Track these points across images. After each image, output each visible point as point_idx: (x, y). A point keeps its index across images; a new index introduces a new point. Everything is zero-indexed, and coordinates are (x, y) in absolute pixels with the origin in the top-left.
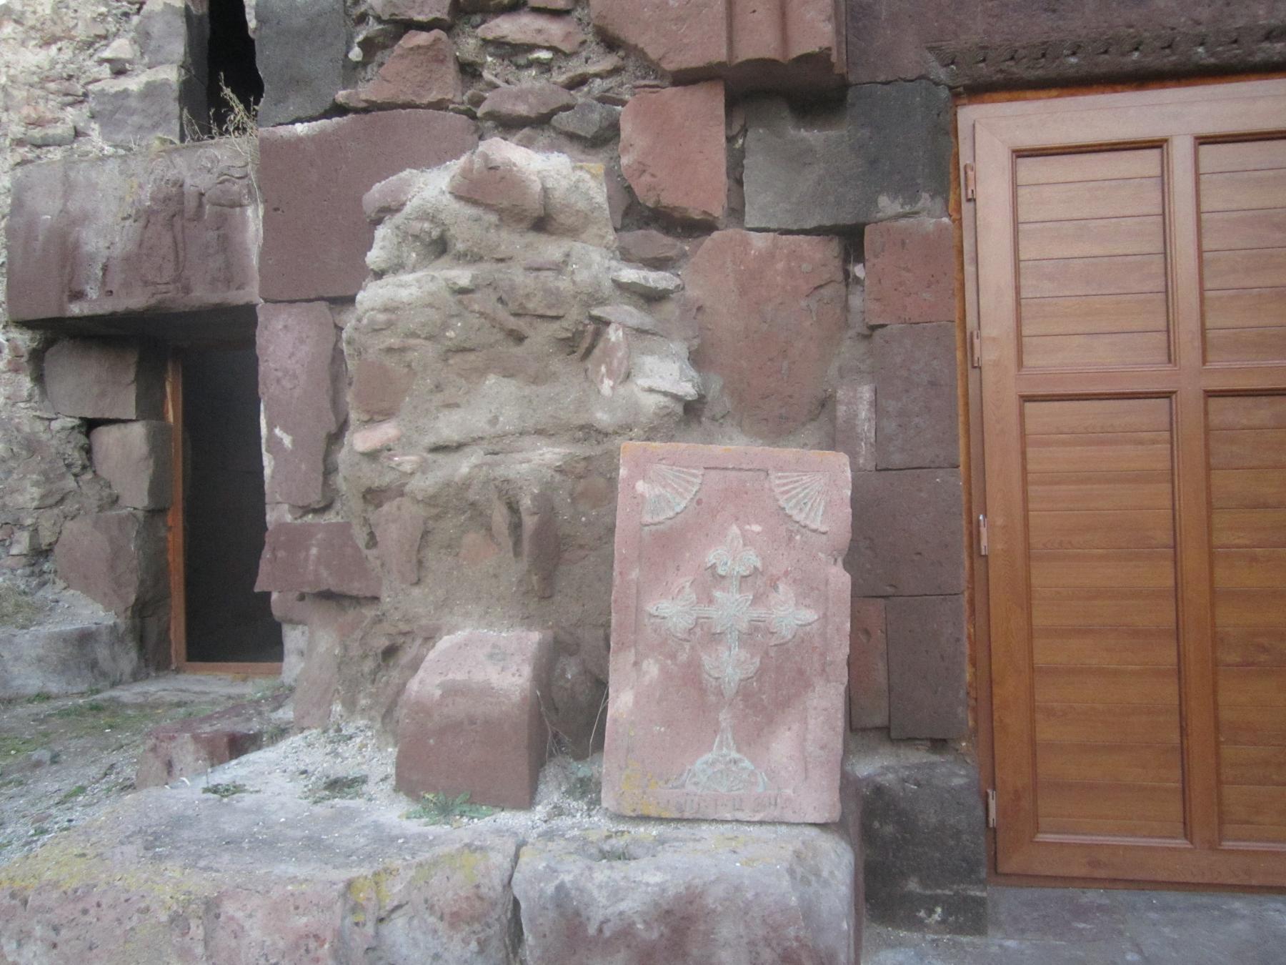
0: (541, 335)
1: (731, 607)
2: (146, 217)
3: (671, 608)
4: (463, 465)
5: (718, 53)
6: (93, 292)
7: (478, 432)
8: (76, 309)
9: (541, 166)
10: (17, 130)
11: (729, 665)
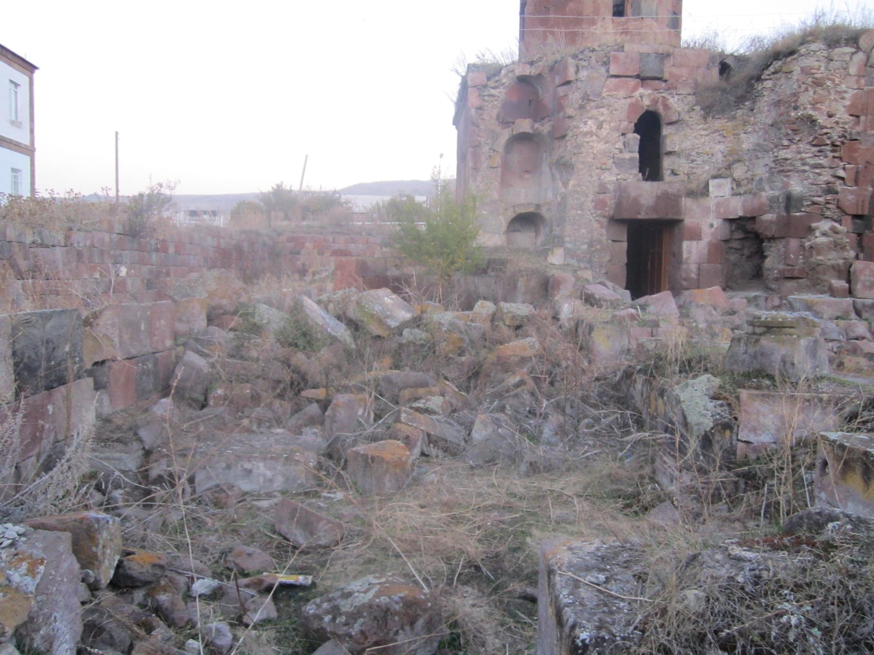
0: (839, 247)
1: (867, 278)
2: (658, 197)
3: (862, 278)
4: (833, 262)
5: (855, 213)
6: (643, 213)
7: (833, 258)
8: (640, 217)
9: (837, 225)
10: (599, 166)
11: (868, 284)
